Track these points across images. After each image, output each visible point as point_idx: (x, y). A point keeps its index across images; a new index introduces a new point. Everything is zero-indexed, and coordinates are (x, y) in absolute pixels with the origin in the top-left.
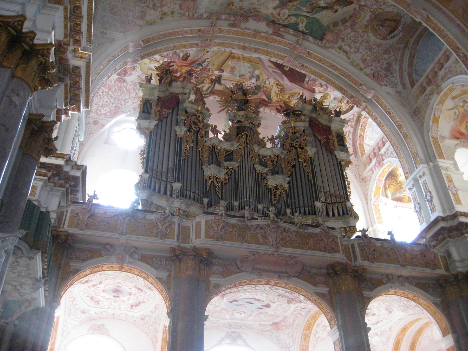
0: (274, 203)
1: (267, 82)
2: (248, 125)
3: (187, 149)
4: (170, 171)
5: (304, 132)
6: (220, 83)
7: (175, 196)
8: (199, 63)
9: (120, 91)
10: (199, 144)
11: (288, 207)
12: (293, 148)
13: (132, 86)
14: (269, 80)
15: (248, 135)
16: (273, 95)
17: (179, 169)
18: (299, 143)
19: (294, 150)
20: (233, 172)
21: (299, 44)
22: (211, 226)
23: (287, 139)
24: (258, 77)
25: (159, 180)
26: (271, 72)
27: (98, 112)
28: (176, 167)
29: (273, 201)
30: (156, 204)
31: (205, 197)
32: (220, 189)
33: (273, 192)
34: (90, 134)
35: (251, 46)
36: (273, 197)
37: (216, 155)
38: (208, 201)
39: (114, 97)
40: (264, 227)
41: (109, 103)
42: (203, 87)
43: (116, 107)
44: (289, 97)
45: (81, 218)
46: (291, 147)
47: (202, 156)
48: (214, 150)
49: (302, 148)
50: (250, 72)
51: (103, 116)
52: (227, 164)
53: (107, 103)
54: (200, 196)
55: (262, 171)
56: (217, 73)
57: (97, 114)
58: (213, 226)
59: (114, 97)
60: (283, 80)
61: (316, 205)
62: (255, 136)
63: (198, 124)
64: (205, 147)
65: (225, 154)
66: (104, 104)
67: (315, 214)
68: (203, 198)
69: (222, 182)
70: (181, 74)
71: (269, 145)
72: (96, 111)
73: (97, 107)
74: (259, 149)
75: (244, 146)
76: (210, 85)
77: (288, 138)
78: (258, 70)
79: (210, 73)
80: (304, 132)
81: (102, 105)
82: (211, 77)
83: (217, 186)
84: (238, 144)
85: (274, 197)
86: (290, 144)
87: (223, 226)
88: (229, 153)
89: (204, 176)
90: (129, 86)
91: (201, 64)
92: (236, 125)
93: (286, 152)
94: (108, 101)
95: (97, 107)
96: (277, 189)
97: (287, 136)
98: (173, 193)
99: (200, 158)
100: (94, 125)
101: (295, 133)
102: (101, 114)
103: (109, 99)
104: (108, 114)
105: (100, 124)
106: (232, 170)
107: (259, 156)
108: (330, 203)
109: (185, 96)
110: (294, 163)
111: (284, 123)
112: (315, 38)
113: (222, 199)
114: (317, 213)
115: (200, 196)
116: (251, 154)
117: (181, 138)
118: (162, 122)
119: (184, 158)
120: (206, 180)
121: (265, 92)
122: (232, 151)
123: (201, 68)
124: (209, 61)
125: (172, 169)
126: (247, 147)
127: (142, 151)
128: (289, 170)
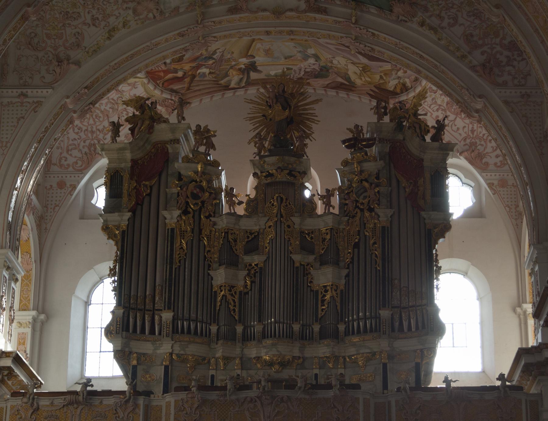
0: (320, 316)
1: (335, 62)
2: (284, 180)
3: (182, 248)
4: (157, 292)
5: (378, 178)
6: (255, 69)
7: (165, 336)
8: (206, 57)
9: (92, 116)
10: (203, 231)
12: (359, 211)
13: (109, 106)
14: (336, 58)
15: (284, 197)
16: (353, 77)
17: (170, 286)
18: (367, 200)
19: (359, 214)
20: (257, 272)
21: (353, 21)
22: (182, 408)
23: (350, 193)
24: (317, 57)
25: (140, 310)
26: (334, 50)
27: (63, 162)
28: (166, 284)
29: (320, 312)
30: (136, 353)
31: (214, 322)
32: (237, 304)
33: (320, 296)
34: (54, 208)
35: (278, 29)
36: (319, 306)
37: (231, 246)
38: (218, 330)
39: (84, 128)
40: (254, 400)
41: (79, 141)
42: (230, 81)
43: (90, 145)
44: (381, 77)
45: (23, 417)
46: (355, 208)
47: (209, 251)
48: (228, 236)
49: (371, 210)
50: (300, 52)
51: (71, 169)
52: (247, 259)
53: (75, 142)
54: (206, 323)
56: (244, 60)
57: (61, 166)
58: (184, 408)
59: (84, 128)
60: (358, 59)
61: (382, 315)
63: (200, 195)
64: (215, 234)
65: (246, 240)
66: (70, 145)
67: (380, 331)
68: (210, 324)
69: (241, 292)
70: (185, 73)
71: (320, 208)
72: (60, 161)
73: (61, 154)
75: (276, 222)
76: (241, 76)
77: (352, 191)
78: (311, 48)
79: (233, 63)
80: (378, 178)
81: (68, 147)
82: (237, 67)
84: (267, 218)
86: (355, 202)
87: (198, 406)
88: (253, 236)
89: (212, 286)
90: (104, 105)
91: (210, 58)
94: (77, 137)
95: (61, 154)
96: (326, 291)
97: (350, 186)
98: (162, 329)
99: (205, 256)
100: (59, 190)
101: (362, 181)
102: (68, 165)
103: (77, 133)
104: (80, 163)
105: (68, 185)
106: (256, 268)
107: (302, 232)
108: (407, 308)
109: (177, 145)
110: (357, 240)
111: (346, 163)
112: (380, 8)
113: (240, 321)
114: (382, 330)
116: (286, 234)
117: (173, 230)
118: (142, 205)
119: (178, 264)
120: (216, 292)
121: (338, 74)
122: (258, 233)
123: (214, 61)
125: (160, 288)
126: (281, 222)
127: (111, 270)
128: (349, 253)
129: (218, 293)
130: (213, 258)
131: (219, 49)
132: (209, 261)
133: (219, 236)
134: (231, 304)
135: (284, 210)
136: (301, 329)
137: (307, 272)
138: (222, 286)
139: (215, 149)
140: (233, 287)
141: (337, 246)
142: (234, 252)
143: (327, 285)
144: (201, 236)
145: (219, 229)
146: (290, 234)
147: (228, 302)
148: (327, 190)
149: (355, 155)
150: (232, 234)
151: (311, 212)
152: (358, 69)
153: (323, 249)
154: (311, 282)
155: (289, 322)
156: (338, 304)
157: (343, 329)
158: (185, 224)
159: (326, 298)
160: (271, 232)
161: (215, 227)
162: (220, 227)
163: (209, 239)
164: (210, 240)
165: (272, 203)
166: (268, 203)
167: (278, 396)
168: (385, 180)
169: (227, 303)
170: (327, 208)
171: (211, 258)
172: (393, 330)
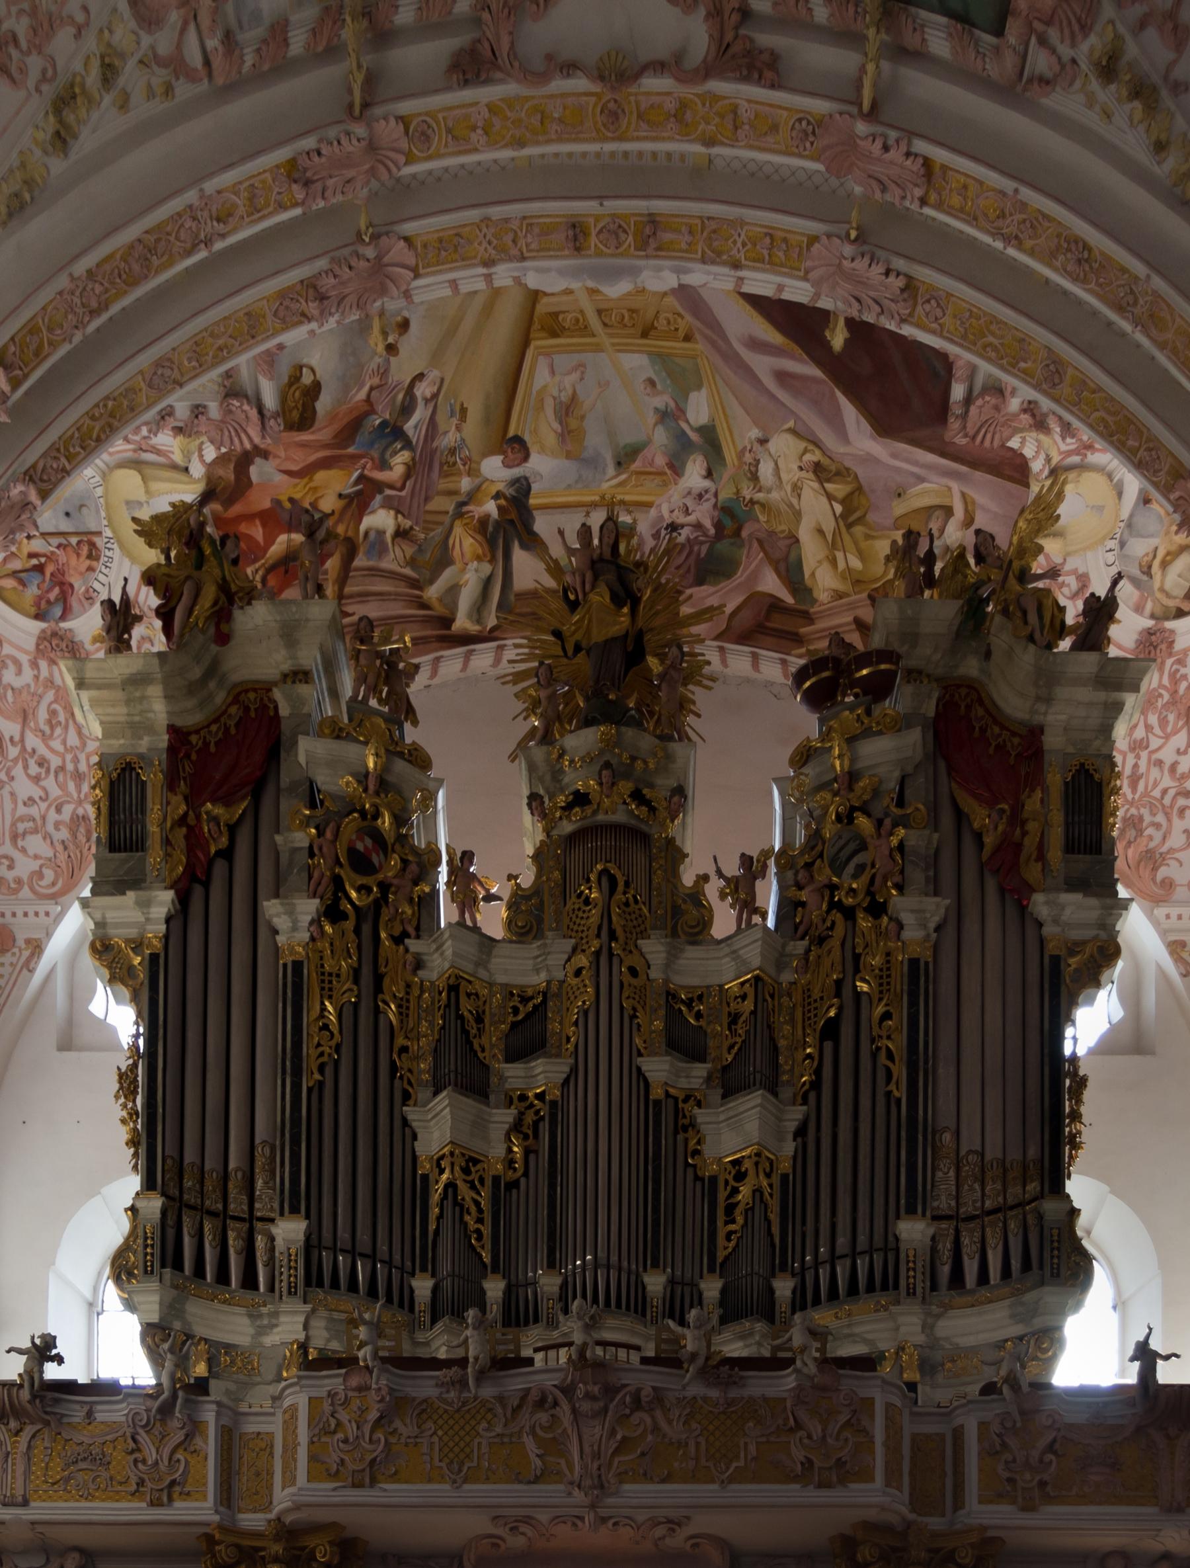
11: (783, 1267)
31: (424, 1269)
36: (720, 1223)
37: (468, 1032)
38: (435, 1290)
47: (404, 1049)
52: (514, 1075)
54: (402, 1269)
55: (683, 1083)
62: (656, 880)
64: (420, 996)
74: (673, 955)
78: (699, 387)
83: (469, 1203)
85: (726, 1223)
92: (567, 827)
93: (800, 946)
96: (740, 1177)
99: (393, 1063)
115: (402, 1269)
122: (545, 994)
124: (435, 396)
128: (809, 1056)
129: (432, 1178)
130: (415, 1071)
131: (420, 376)
132: (405, 1082)
133: (433, 1003)
134: (469, 1214)
135: (619, 915)
136: (669, 1289)
137: (686, 1122)
138: (442, 1157)
139: (415, 723)
140: (476, 1162)
141: (772, 1039)
142: (475, 1052)
143: (743, 1157)
144: (380, 996)
145: (432, 983)
146: (637, 997)
147: (462, 1206)
148: (743, 855)
149: (832, 723)
150: (469, 995)
151: (696, 930)
152: (828, 506)
153: (731, 1047)
154: (696, 1153)
155: (634, 1267)
156: (772, 1216)
157: (788, 1293)
158: (332, 951)
159: (740, 1197)
160: (582, 990)
161: (420, 973)
162: (434, 976)
163: (404, 1010)
164: (407, 1015)
165: (583, 897)
166: (574, 899)
167: (626, 1385)
168: (921, 806)
169: (457, 1209)
170: (745, 916)
171: (410, 1071)
172: (934, 1287)
